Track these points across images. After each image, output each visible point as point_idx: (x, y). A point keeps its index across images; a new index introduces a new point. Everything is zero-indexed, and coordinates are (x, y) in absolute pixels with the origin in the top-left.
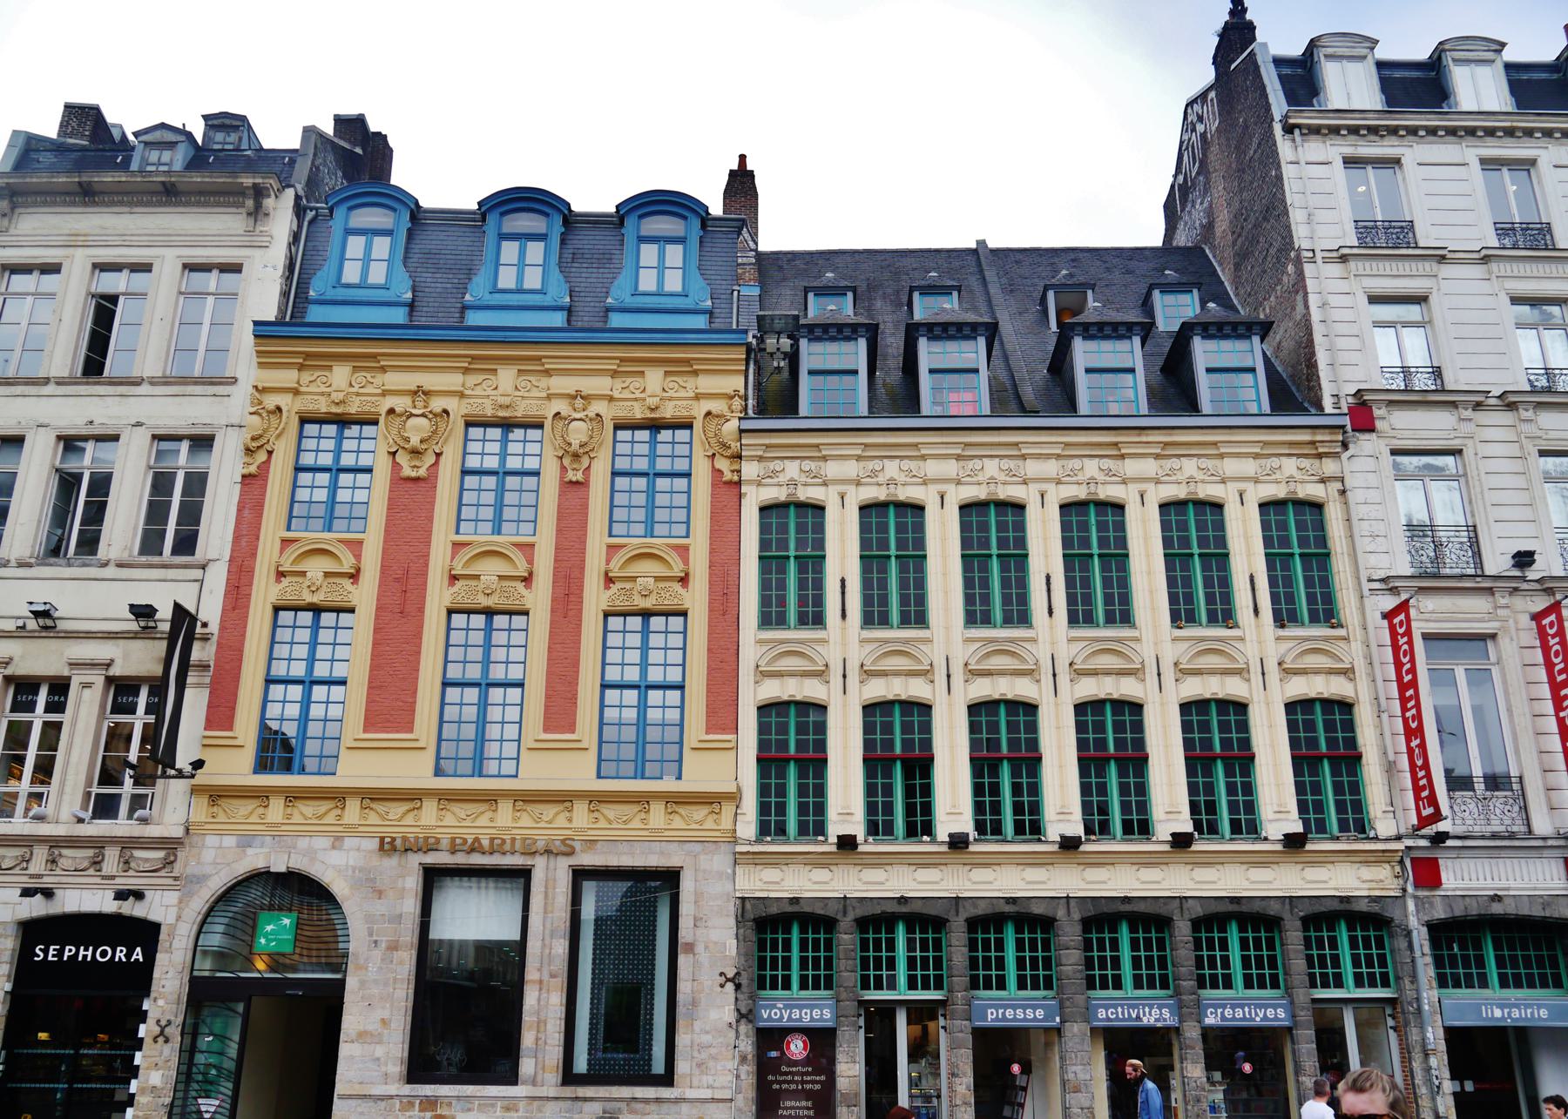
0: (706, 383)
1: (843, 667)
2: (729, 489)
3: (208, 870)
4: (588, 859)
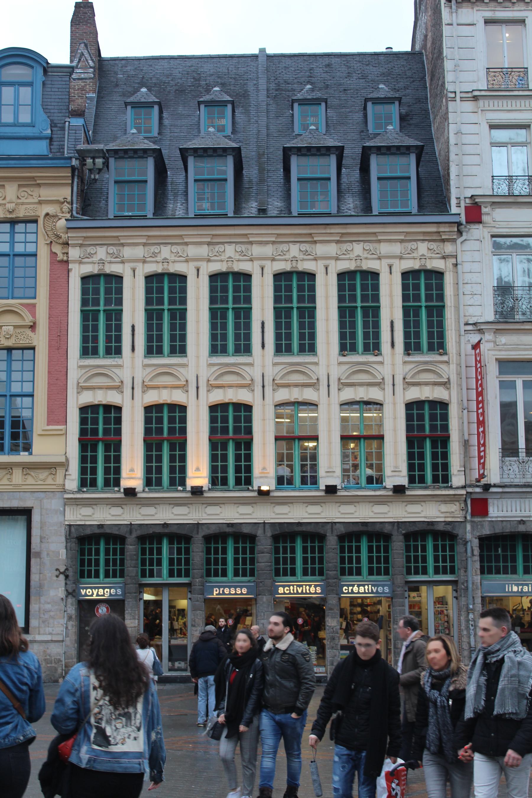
0: (46, 193)
1: (132, 382)
2: (60, 266)
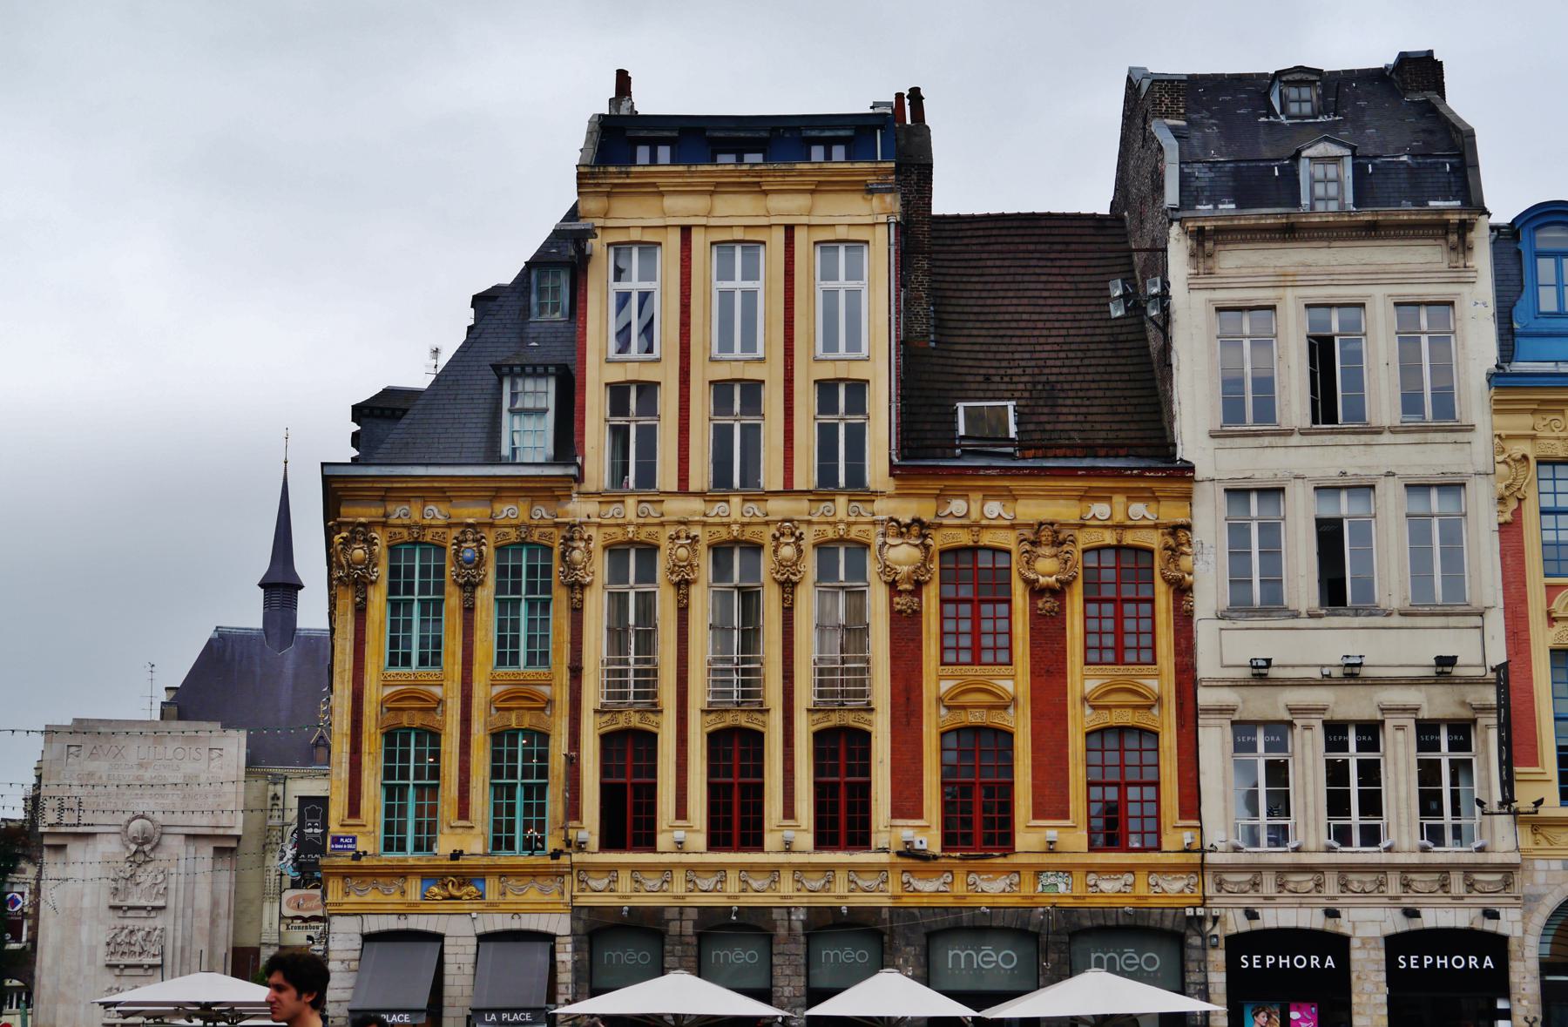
3: (1542, 890)
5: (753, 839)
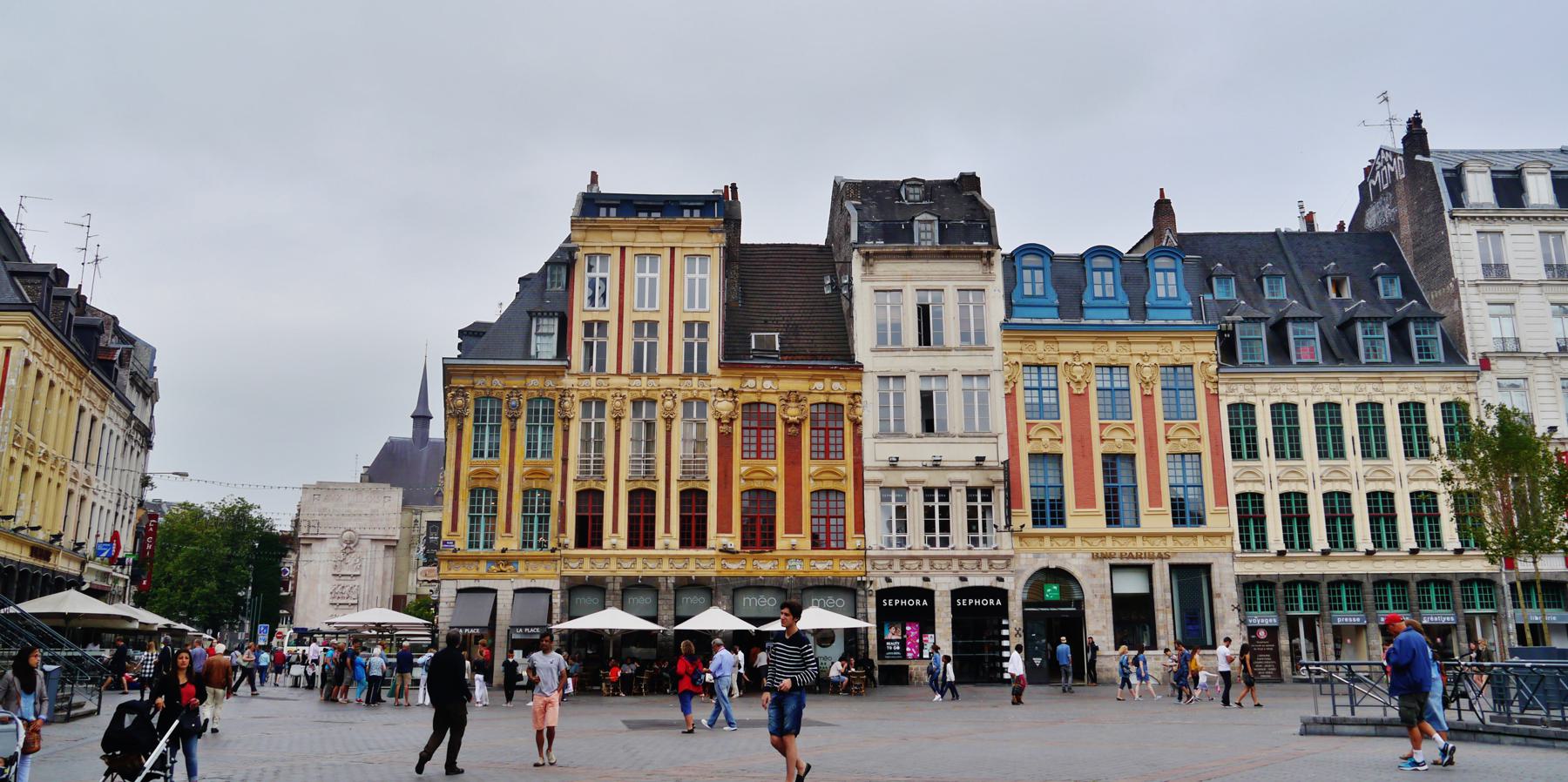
0: (1200, 347)
1: (1269, 476)
2: (1213, 398)
4: (1175, 560)
5: (650, 543)
